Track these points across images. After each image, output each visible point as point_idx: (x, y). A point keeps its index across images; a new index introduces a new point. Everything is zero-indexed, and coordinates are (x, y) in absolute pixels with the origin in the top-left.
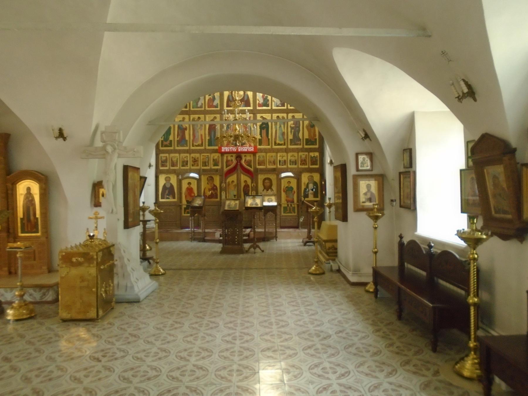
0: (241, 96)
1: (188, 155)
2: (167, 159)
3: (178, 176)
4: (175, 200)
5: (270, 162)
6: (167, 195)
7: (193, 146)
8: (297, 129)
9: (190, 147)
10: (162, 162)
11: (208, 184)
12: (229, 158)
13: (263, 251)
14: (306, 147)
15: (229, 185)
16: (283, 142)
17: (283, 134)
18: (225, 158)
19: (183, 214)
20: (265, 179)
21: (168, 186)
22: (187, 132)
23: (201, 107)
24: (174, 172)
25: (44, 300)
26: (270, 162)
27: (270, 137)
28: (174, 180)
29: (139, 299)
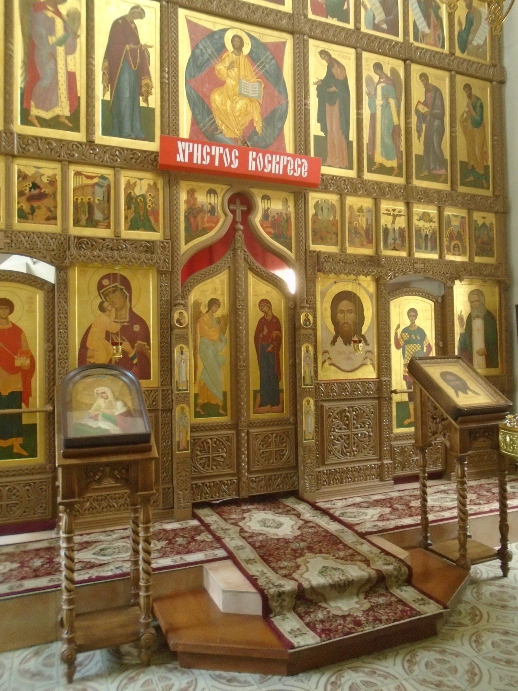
8: (437, 122)
11: (102, 308)
12: (202, 198)
14: (462, 189)
16: (393, 163)
17: (395, 131)
18: (183, 196)
26: (355, 231)
27: (353, 136)
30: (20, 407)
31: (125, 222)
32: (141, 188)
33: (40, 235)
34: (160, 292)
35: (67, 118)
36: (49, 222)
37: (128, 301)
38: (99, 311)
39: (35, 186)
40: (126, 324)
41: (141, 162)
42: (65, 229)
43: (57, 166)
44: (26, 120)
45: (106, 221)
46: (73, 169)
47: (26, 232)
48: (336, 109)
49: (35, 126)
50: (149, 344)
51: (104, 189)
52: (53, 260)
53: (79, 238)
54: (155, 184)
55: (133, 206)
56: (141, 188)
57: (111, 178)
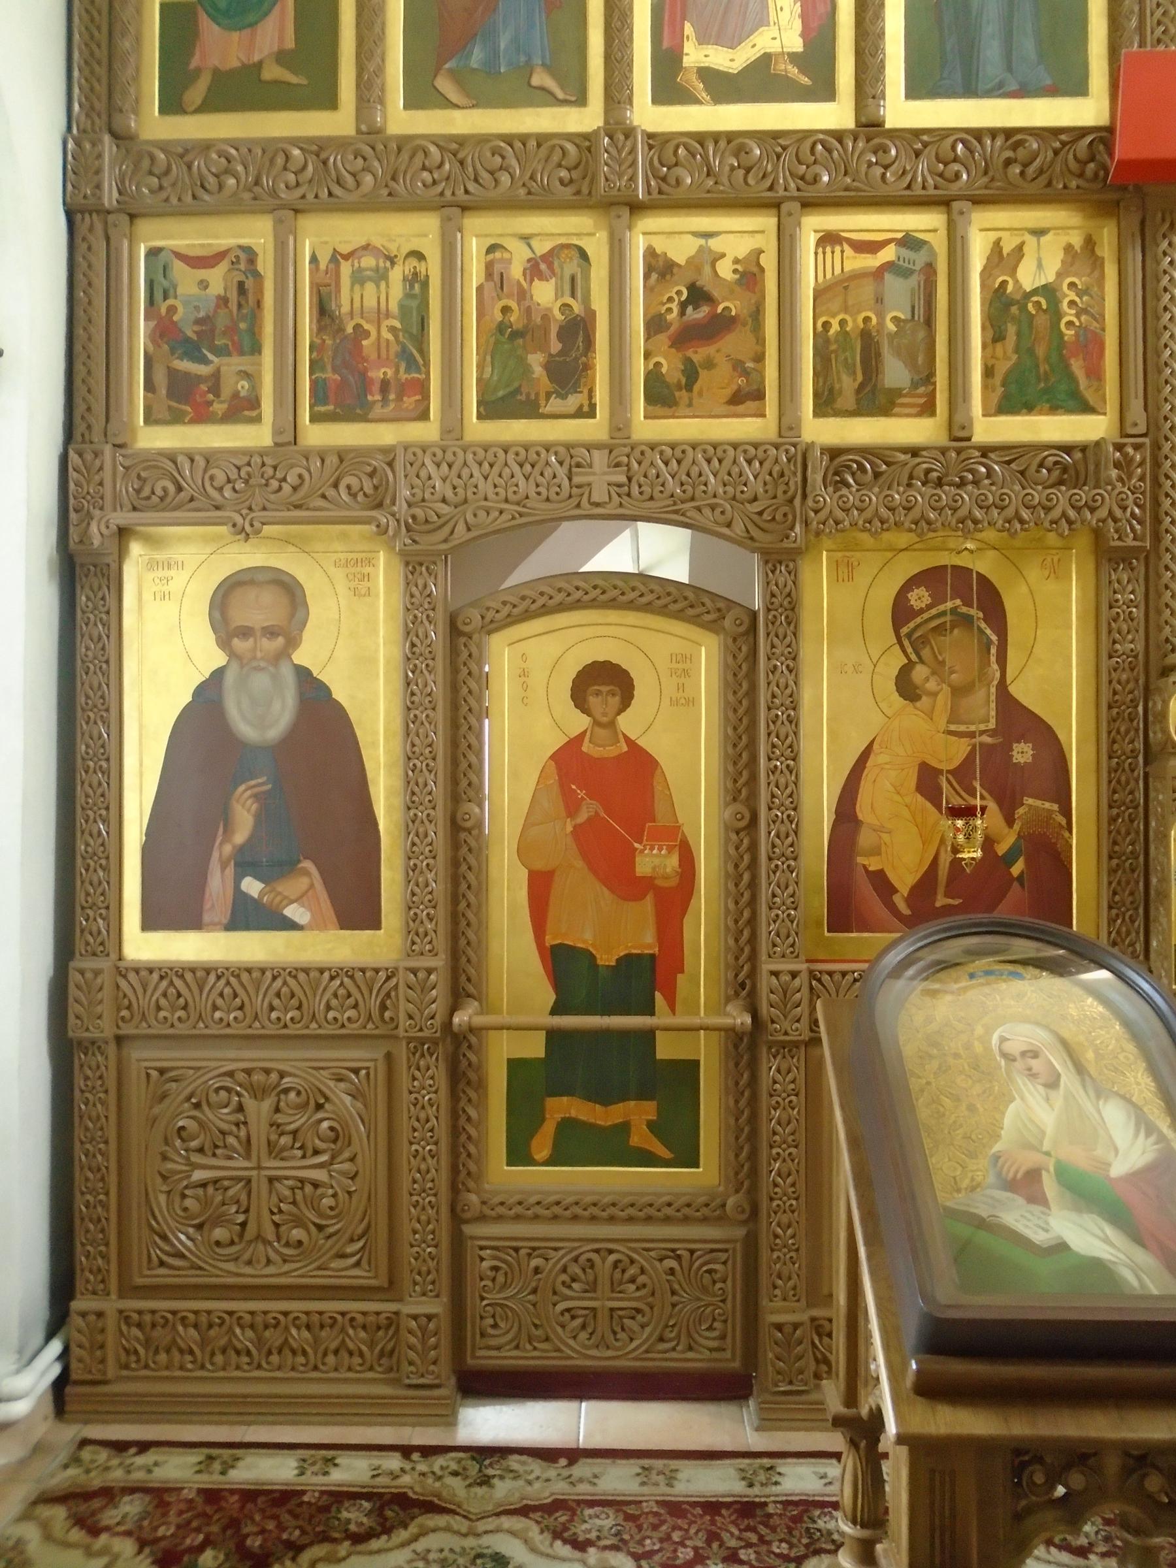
1: (583, 228)
2: (245, 292)
4: (377, 947)
6: (245, 864)
7: (669, 88)
9: (617, 92)
11: (906, 687)
19: (502, 1175)
24: (364, 492)
28: (355, 637)
30: (649, 1009)
31: (985, 387)
32: (1040, 266)
33: (715, 451)
34: (1105, 622)
35: (794, 57)
36: (740, 408)
37: (993, 659)
38: (896, 696)
39: (697, 295)
40: (986, 739)
41: (1041, 172)
42: (788, 425)
43: (766, 222)
44: (669, 88)
45: (922, 390)
46: (812, 225)
47: (673, 446)
49: (697, 102)
50: (1067, 812)
51: (913, 281)
52: (755, 532)
53: (834, 453)
54: (1090, 243)
55: (1011, 330)
56: (1040, 266)
57: (939, 242)
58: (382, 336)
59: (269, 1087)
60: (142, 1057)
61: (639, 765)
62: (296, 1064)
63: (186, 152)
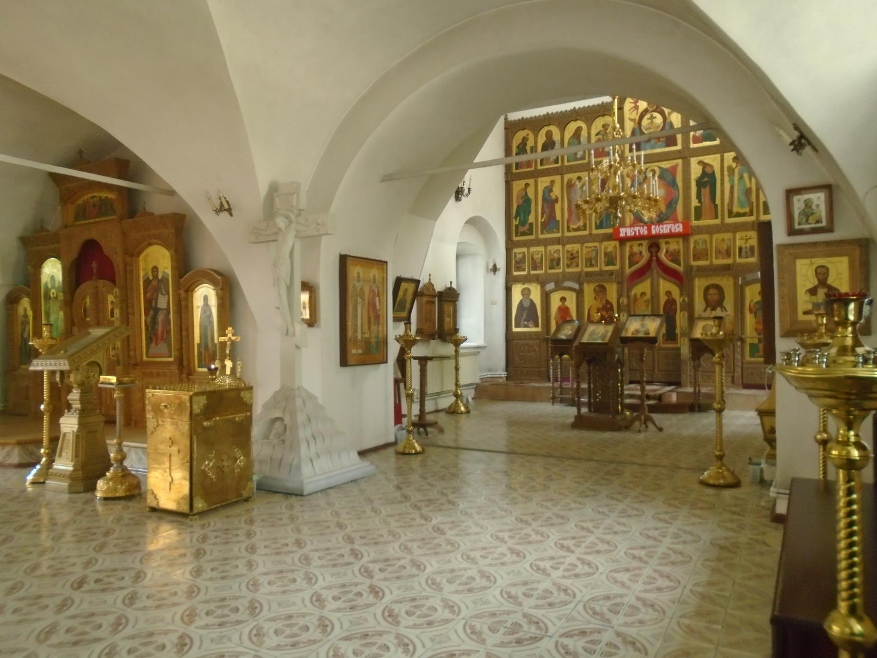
0: (658, 126)
1: (560, 247)
2: (524, 256)
3: (542, 287)
4: (539, 329)
5: (719, 252)
7: (569, 230)
9: (563, 232)
10: (516, 262)
11: (595, 299)
12: (636, 249)
13: (661, 429)
15: (636, 300)
16: (747, 210)
17: (748, 192)
20: (707, 289)
21: (527, 304)
22: (558, 206)
23: (583, 158)
24: (537, 279)
25: (8, 462)
26: (719, 252)
27: (718, 201)
28: (536, 296)
29: (302, 491)
44: (569, 230)
48: (708, 189)
58: (538, 261)
59: (528, 345)
60: (515, 342)
61: (567, 308)
62: (531, 342)
63: (518, 241)
